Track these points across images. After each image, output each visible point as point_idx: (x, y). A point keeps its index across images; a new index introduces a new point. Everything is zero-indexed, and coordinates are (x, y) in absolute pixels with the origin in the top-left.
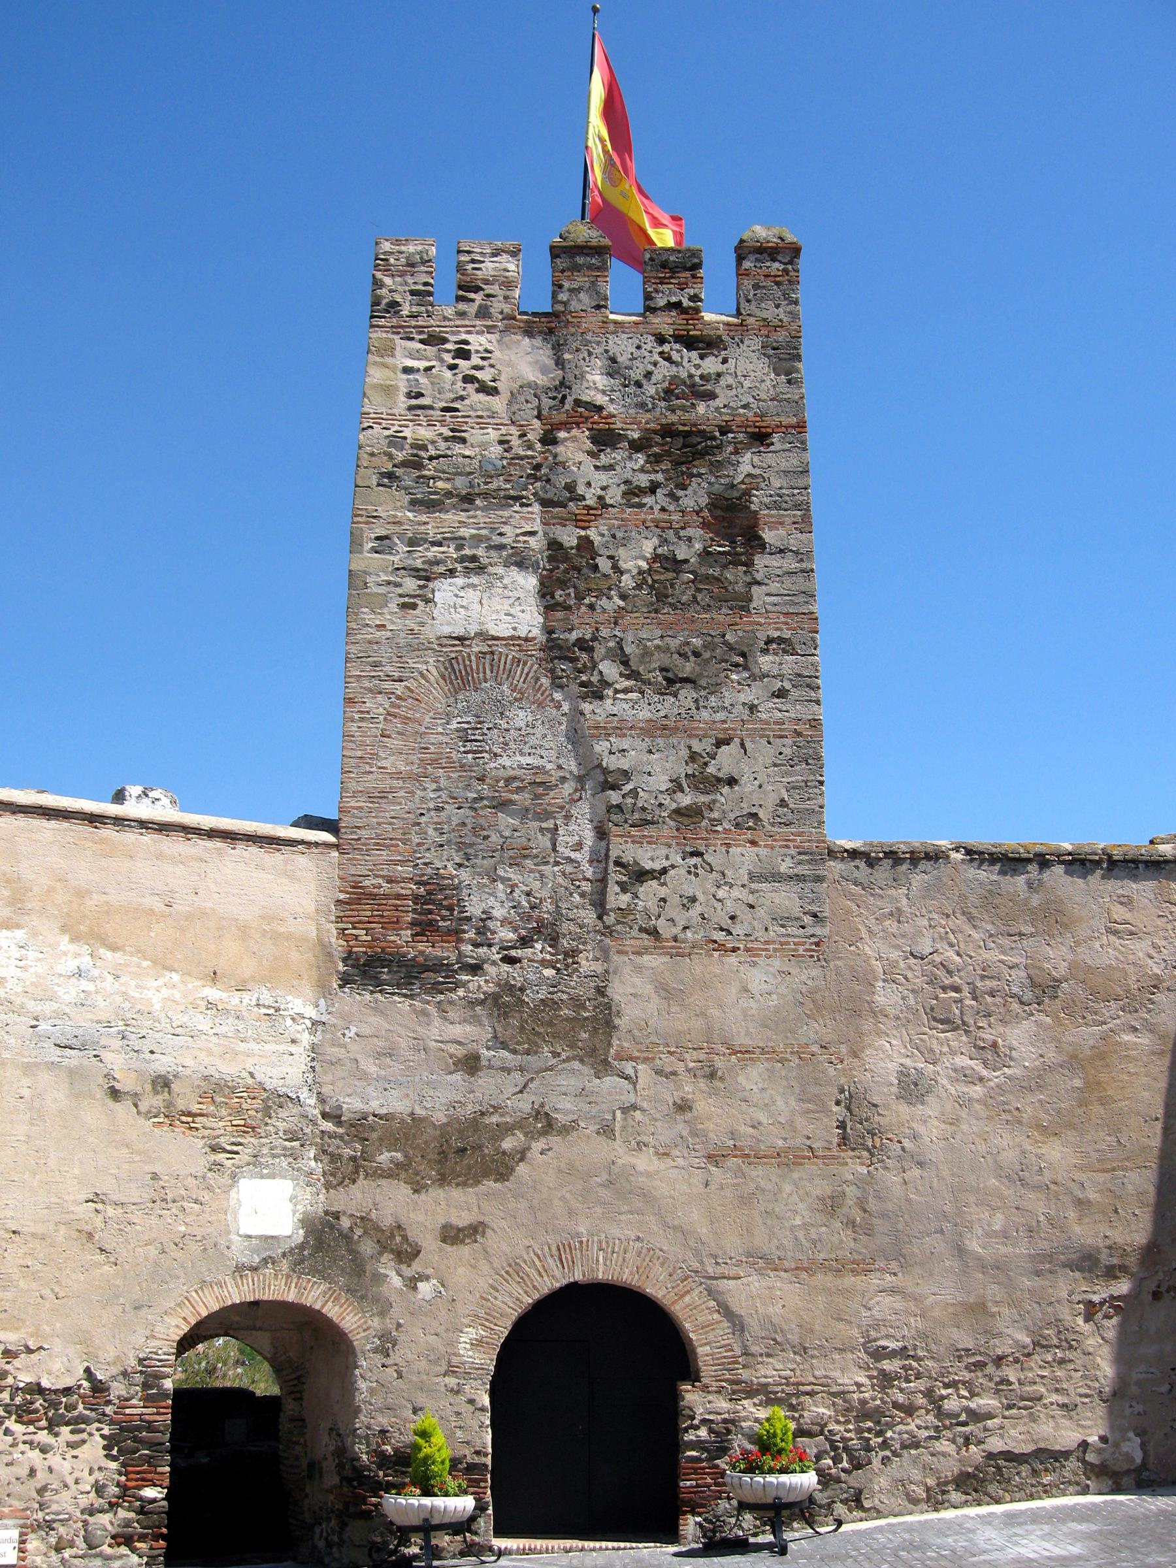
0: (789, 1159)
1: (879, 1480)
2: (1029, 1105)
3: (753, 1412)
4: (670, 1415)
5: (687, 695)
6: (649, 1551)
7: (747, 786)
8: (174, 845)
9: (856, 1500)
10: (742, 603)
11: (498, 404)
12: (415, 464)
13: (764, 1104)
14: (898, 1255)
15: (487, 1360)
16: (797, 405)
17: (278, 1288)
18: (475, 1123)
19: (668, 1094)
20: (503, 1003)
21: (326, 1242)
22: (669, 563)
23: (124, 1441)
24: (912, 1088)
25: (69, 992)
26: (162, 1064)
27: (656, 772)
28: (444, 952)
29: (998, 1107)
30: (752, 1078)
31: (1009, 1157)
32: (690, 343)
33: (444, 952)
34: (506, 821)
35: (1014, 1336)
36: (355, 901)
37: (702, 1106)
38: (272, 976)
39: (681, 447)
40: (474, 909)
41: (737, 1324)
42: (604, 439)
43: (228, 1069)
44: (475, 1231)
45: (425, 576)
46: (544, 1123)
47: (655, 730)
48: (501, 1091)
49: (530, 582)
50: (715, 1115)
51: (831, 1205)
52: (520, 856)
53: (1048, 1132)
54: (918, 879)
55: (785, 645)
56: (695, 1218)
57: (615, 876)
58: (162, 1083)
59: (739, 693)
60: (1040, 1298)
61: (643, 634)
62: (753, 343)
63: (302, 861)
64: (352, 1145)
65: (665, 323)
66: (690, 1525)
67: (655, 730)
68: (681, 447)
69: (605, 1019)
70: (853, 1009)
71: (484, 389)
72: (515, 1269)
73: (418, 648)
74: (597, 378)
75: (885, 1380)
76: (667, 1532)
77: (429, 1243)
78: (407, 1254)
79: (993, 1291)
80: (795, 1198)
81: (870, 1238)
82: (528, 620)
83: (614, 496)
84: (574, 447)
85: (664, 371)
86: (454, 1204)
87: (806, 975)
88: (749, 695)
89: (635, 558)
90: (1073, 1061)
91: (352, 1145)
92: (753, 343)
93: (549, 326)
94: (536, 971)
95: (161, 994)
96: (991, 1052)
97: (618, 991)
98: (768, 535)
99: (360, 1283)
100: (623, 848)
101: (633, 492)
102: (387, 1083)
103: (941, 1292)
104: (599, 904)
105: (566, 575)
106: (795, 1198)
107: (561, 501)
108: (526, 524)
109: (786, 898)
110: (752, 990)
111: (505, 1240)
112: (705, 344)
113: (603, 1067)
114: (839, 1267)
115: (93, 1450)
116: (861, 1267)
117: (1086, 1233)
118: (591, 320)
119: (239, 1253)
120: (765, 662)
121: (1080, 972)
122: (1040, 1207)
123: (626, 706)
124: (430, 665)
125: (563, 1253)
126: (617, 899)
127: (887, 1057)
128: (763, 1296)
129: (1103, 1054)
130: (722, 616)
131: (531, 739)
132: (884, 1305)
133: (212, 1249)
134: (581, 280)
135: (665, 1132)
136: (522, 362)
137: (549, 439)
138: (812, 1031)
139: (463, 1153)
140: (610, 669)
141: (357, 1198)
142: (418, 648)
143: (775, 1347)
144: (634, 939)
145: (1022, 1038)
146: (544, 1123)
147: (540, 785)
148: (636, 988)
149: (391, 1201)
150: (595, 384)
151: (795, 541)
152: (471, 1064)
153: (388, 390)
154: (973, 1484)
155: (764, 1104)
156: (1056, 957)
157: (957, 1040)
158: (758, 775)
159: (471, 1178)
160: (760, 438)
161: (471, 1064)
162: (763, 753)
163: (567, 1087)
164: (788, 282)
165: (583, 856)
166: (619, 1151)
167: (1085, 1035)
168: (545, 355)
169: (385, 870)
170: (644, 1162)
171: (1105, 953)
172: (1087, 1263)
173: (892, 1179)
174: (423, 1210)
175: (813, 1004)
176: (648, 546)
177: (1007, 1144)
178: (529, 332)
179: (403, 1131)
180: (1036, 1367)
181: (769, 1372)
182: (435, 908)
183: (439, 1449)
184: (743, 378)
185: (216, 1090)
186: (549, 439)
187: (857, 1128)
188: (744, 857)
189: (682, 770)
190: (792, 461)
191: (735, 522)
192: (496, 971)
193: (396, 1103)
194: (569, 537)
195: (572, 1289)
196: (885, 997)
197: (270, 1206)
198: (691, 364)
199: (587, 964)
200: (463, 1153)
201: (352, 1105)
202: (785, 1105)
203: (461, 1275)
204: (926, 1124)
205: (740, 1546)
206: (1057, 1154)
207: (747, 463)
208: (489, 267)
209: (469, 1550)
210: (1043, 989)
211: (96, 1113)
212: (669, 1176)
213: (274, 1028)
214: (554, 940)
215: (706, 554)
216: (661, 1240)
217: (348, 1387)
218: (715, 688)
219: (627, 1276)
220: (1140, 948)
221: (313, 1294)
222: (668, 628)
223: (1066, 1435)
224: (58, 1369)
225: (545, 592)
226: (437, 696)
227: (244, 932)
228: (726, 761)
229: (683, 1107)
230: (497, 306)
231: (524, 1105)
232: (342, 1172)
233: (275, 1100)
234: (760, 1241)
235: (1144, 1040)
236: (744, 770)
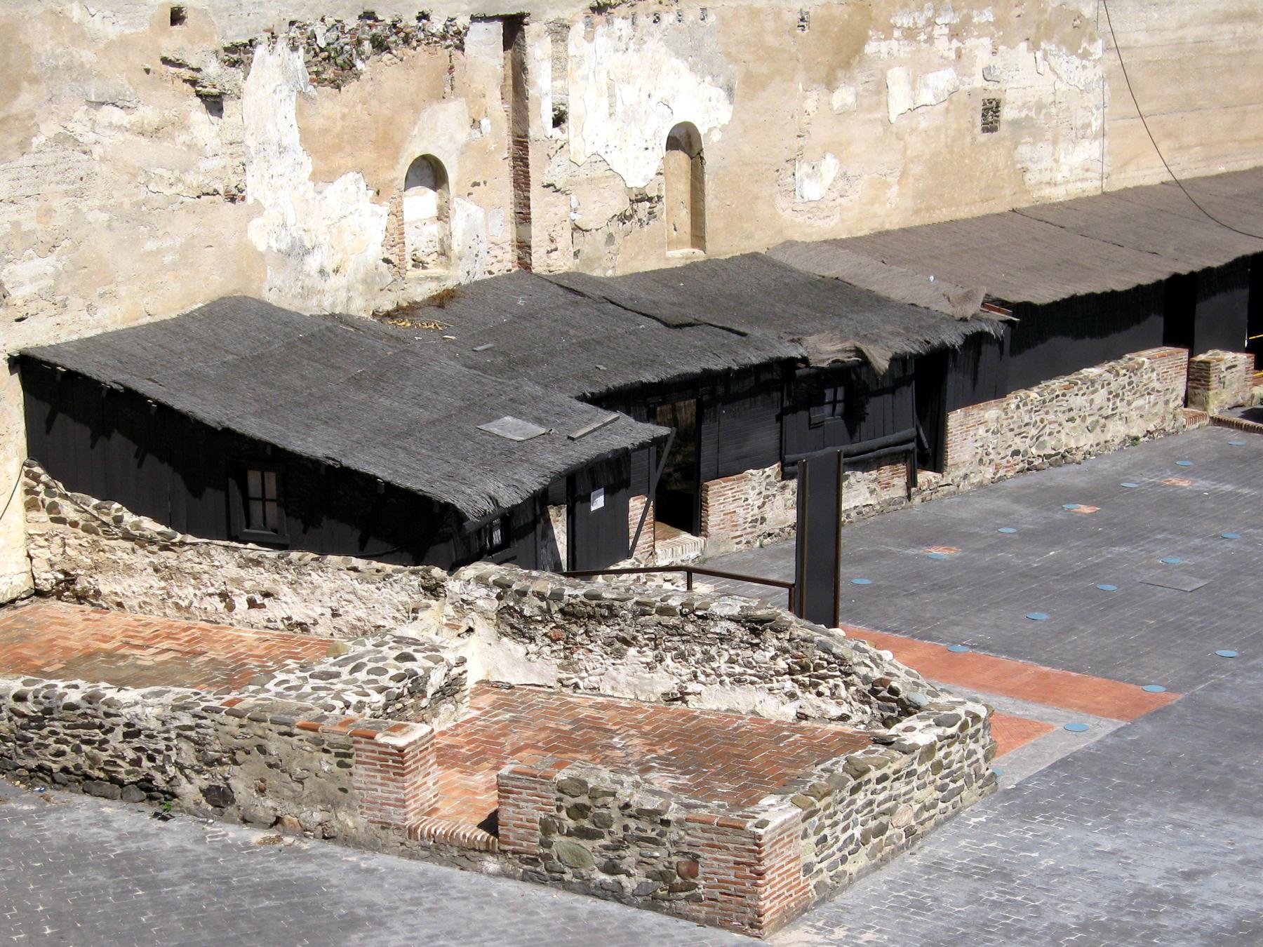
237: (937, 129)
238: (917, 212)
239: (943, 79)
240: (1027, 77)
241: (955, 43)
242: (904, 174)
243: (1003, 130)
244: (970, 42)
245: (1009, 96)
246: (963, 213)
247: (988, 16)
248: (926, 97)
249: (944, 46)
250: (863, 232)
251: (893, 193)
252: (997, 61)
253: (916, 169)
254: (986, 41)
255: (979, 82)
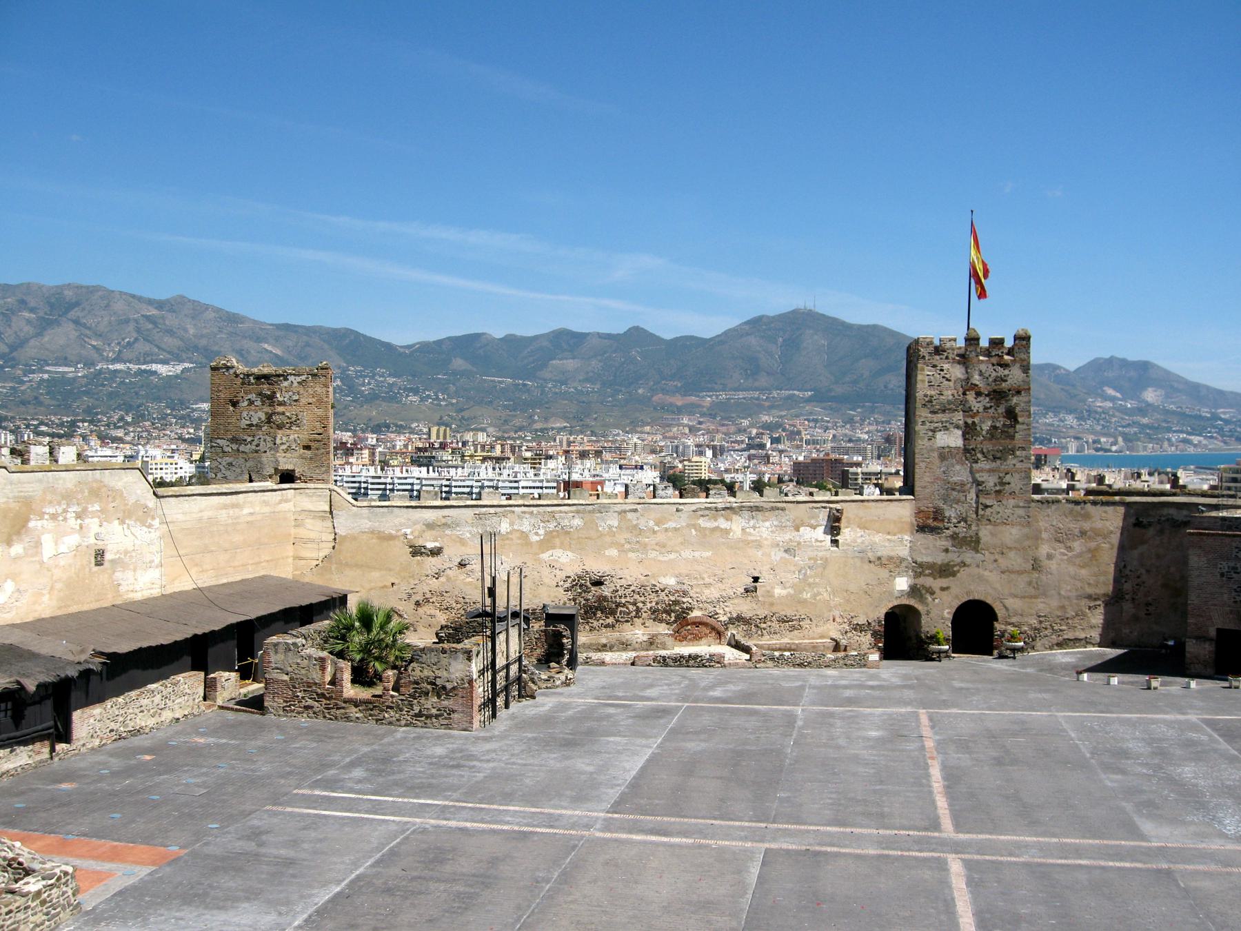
0: (1020, 573)
1: (1038, 644)
2: (1078, 561)
3: (1010, 628)
4: (992, 628)
5: (998, 462)
6: (986, 657)
7: (1013, 485)
8: (879, 504)
9: (1033, 648)
10: (1012, 438)
11: (951, 384)
12: (930, 401)
13: (1015, 560)
14: (1045, 594)
15: (951, 617)
16: (1028, 383)
17: (905, 601)
18: (948, 564)
19: (992, 558)
20: (954, 537)
21: (914, 591)
22: (994, 427)
23: (875, 634)
24: (1050, 557)
25: (859, 541)
26: (879, 554)
27: (990, 481)
28: (940, 525)
29: (1070, 561)
30: (1012, 554)
31: (1072, 573)
32: (1001, 365)
33: (940, 525)
34: (955, 493)
35: (1071, 613)
36: (919, 512)
37: (1000, 561)
38: (900, 532)
39: (998, 395)
40: (947, 514)
41: (1007, 609)
42: (979, 394)
43: (892, 554)
44: (948, 588)
45: (934, 431)
46: (964, 564)
47: (991, 471)
48: (954, 557)
49: (960, 433)
50: (1003, 562)
51: (1030, 583)
52: (958, 502)
53: (1082, 567)
54: (1054, 507)
55: (1023, 449)
56: (998, 586)
57: (981, 507)
58: (879, 558)
59: (1011, 460)
60: (1078, 605)
61: (988, 446)
62: (1018, 365)
63: (907, 504)
64: (920, 569)
65: (994, 360)
66: (995, 652)
67: (991, 471)
68: (998, 395)
69: (978, 541)
70: (1037, 538)
71: (948, 380)
72: (957, 597)
73: (933, 450)
74: (977, 377)
75: (1041, 622)
76: (991, 654)
77: (938, 591)
78: (932, 593)
79: (1067, 603)
80: (1021, 582)
81: (1039, 591)
82: (959, 443)
83: (981, 410)
84: (971, 396)
85: (994, 374)
86: (943, 582)
87: (1026, 530)
88: (1014, 462)
89: (986, 426)
90: (1090, 551)
91: (920, 569)
92: (1018, 365)
93: (963, 359)
94: (962, 529)
95: (877, 538)
96: (1069, 548)
97: (981, 534)
98: (1020, 420)
99: (922, 599)
100: (982, 500)
101: (986, 408)
102: (927, 555)
103: (1055, 603)
104: (977, 513)
105: (969, 431)
106: (1021, 582)
107: (967, 411)
108: (959, 417)
109: (1021, 512)
110: (1012, 534)
111: (955, 590)
112: (1005, 366)
113: (977, 551)
114: (1031, 597)
115: (869, 636)
116: (1036, 597)
117: (1089, 590)
118: (975, 360)
119: (896, 594)
120: (1018, 453)
121: (1091, 529)
122: (1079, 584)
123: (984, 464)
124: (936, 454)
125: (968, 593)
126: (981, 512)
127: (1044, 549)
128: (1012, 603)
129: (1097, 549)
130: (1008, 441)
131: (960, 473)
132: (1041, 606)
133: (891, 593)
134: (972, 348)
135: (991, 567)
136: (957, 372)
137: (964, 394)
138: (1027, 543)
139: (945, 571)
140: (979, 456)
141: (921, 581)
142: (933, 450)
143: (1016, 614)
144: (984, 522)
145: (1077, 545)
146: (964, 564)
147: (963, 485)
148: (985, 533)
149: (928, 581)
150: (976, 379)
151: (1026, 421)
152: (947, 551)
153: (923, 381)
154: (1060, 645)
155: (1015, 560)
156: (1086, 525)
157: (1061, 545)
158: (1015, 482)
159: (947, 576)
160: (1019, 392)
161: (947, 551)
162: (1017, 476)
163: (969, 556)
164: (1028, 347)
165: (973, 502)
166: (981, 571)
167: (1093, 545)
168: (963, 370)
169: (928, 505)
170: (986, 573)
171: (1099, 525)
172: (1090, 597)
173: (1044, 578)
174: (936, 584)
175: (1027, 537)
176: (989, 423)
177: (1072, 569)
178: (959, 363)
179: (931, 566)
180: (1076, 620)
181: (1014, 620)
182: (938, 514)
183: (941, 636)
184: (1015, 375)
185: (890, 558)
186: (964, 394)
187: (1036, 566)
188: (1012, 502)
189: (997, 481)
190: (1025, 399)
191: (1011, 414)
192: (953, 529)
193: (929, 559)
194: (970, 421)
195: (969, 601)
196: (1044, 535)
197: (902, 583)
198: (1002, 372)
199: (974, 528)
200: (945, 571)
201: (919, 560)
202: (1019, 560)
203: (945, 598)
204: (1053, 565)
205: (1006, 657)
206: (1084, 572)
207: (1015, 400)
208: (948, 345)
209: (948, 657)
210: (1083, 533)
211: (867, 566)
212: (992, 576)
213: (902, 544)
214: (966, 522)
215: (1004, 425)
216: (991, 591)
217: (919, 622)
218: (1005, 460)
219: (982, 598)
220: (1108, 524)
221: (912, 602)
222: (994, 445)
223: (1082, 635)
224: (862, 620)
225: (964, 435)
226: (937, 462)
227: (895, 522)
228: (1008, 478)
229: (996, 561)
230: (950, 356)
231: (958, 560)
232: (917, 575)
233: (903, 559)
234: (1013, 591)
235: (1107, 546)
236: (1012, 480)
237: (70, 565)
238: (59, 608)
239: (73, 540)
240: (117, 538)
241: (79, 521)
242: (52, 588)
243: (106, 564)
244: (87, 521)
245: (109, 547)
246: (86, 608)
247: (97, 507)
248: (63, 548)
249: (73, 523)
250: (30, 619)
251: (46, 598)
252: (102, 530)
253: (59, 586)
254: (96, 520)
255: (92, 541)
